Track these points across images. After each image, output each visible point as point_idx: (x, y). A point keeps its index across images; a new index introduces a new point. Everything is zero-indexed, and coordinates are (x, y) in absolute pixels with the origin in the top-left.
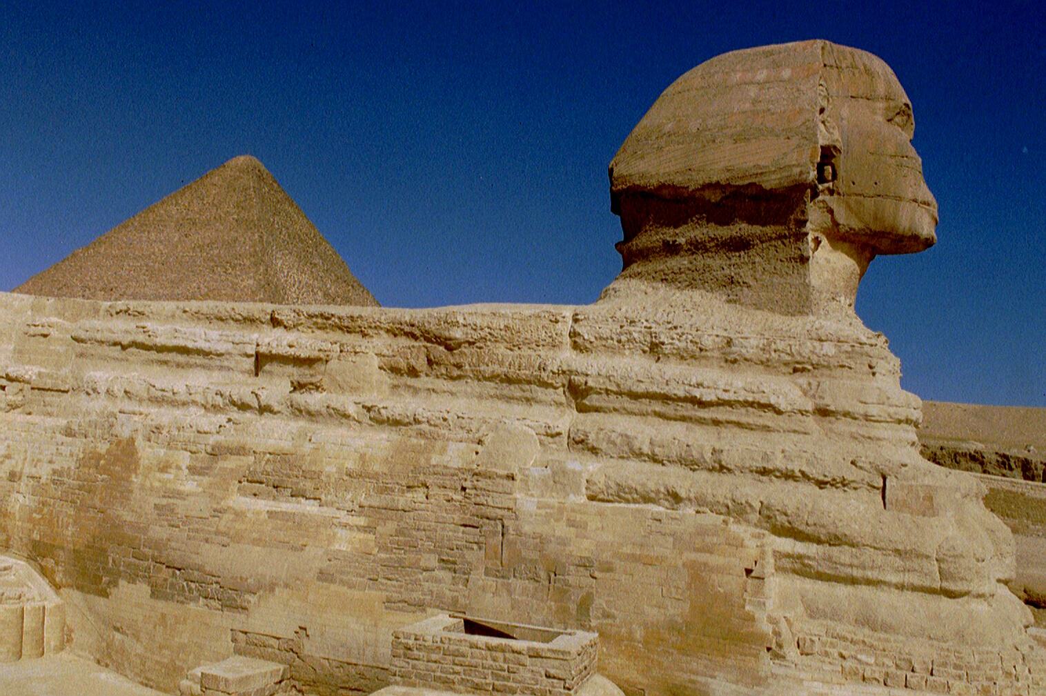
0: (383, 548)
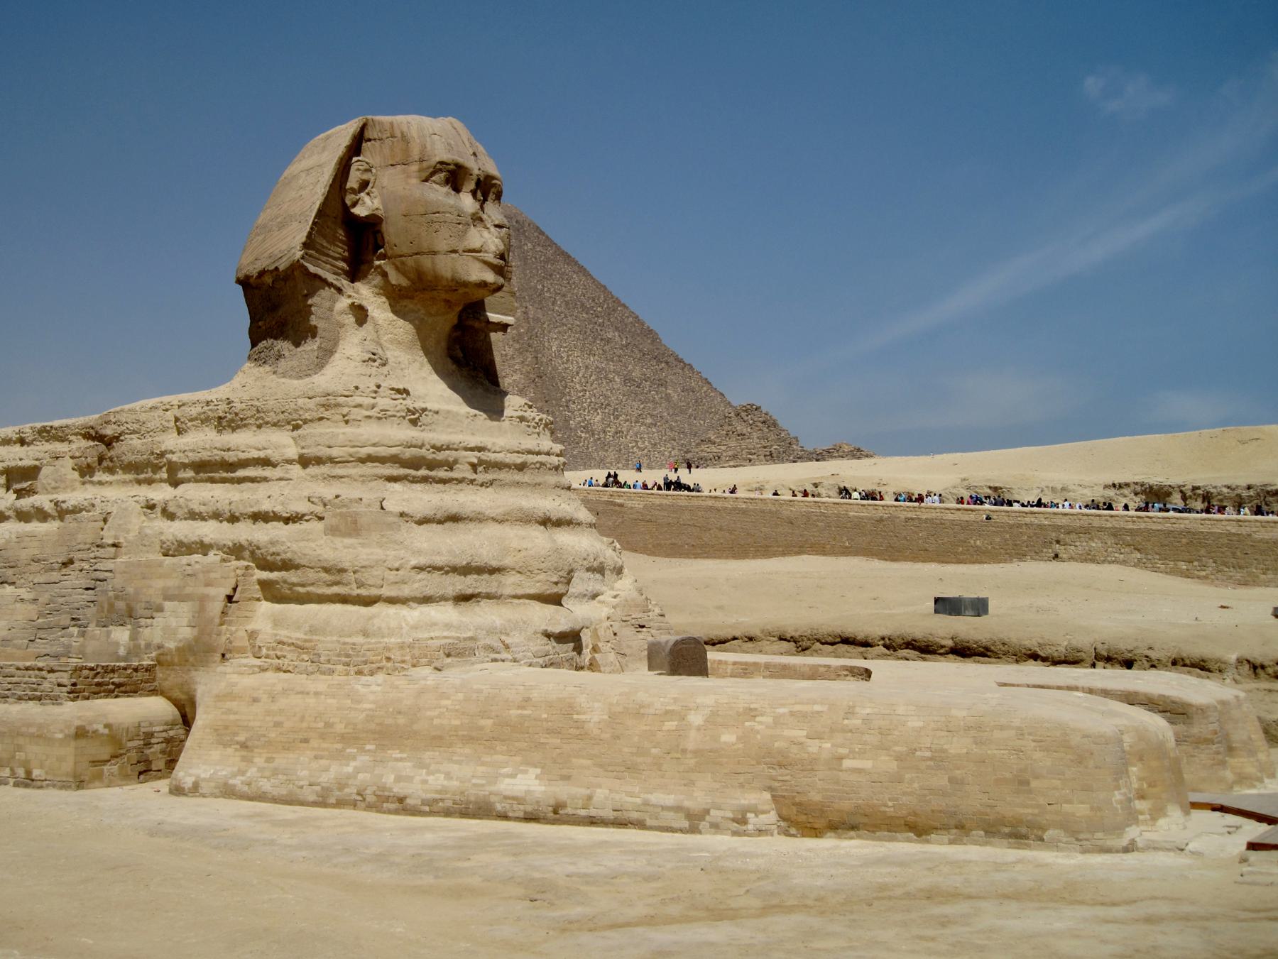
0: (40, 615)
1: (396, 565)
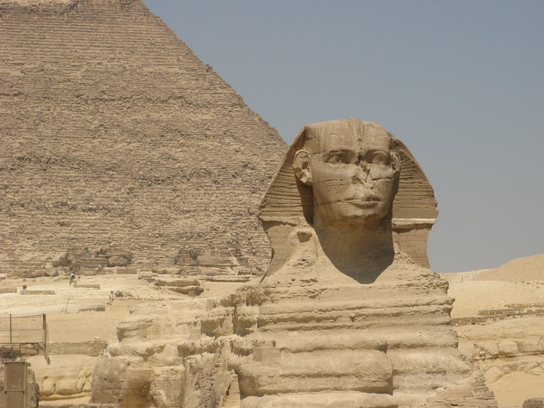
1: (272, 375)
